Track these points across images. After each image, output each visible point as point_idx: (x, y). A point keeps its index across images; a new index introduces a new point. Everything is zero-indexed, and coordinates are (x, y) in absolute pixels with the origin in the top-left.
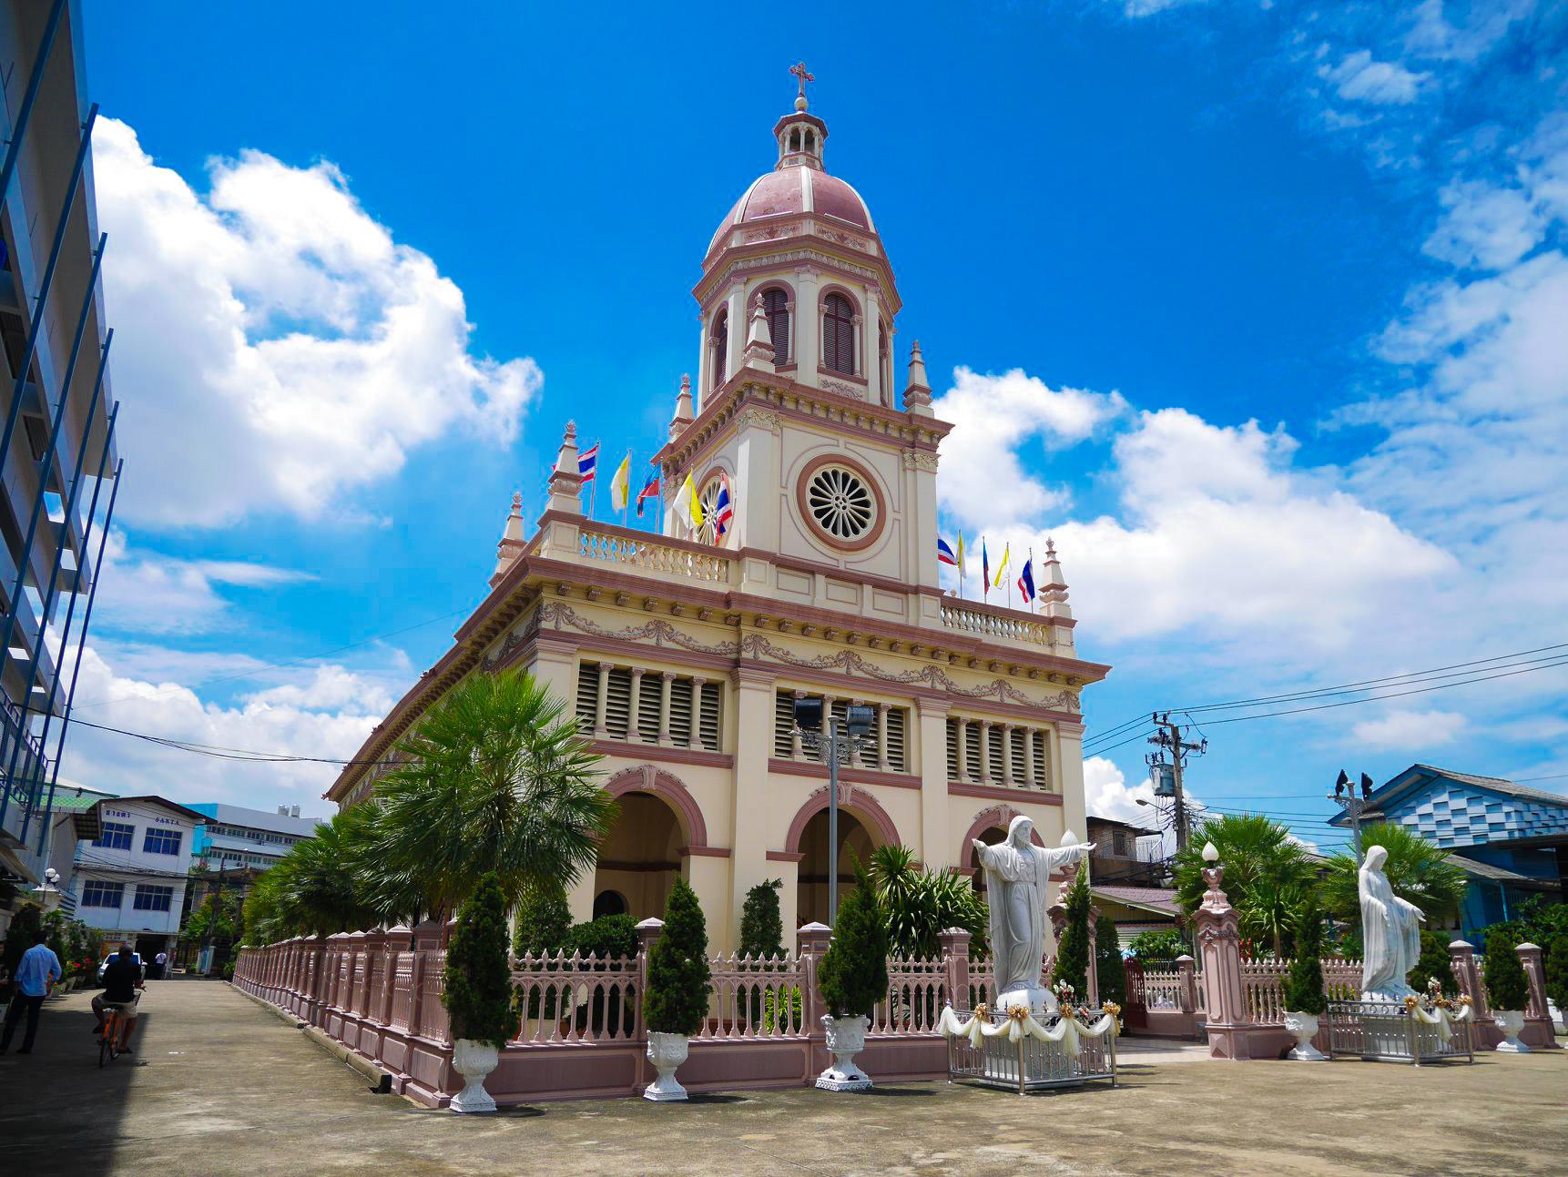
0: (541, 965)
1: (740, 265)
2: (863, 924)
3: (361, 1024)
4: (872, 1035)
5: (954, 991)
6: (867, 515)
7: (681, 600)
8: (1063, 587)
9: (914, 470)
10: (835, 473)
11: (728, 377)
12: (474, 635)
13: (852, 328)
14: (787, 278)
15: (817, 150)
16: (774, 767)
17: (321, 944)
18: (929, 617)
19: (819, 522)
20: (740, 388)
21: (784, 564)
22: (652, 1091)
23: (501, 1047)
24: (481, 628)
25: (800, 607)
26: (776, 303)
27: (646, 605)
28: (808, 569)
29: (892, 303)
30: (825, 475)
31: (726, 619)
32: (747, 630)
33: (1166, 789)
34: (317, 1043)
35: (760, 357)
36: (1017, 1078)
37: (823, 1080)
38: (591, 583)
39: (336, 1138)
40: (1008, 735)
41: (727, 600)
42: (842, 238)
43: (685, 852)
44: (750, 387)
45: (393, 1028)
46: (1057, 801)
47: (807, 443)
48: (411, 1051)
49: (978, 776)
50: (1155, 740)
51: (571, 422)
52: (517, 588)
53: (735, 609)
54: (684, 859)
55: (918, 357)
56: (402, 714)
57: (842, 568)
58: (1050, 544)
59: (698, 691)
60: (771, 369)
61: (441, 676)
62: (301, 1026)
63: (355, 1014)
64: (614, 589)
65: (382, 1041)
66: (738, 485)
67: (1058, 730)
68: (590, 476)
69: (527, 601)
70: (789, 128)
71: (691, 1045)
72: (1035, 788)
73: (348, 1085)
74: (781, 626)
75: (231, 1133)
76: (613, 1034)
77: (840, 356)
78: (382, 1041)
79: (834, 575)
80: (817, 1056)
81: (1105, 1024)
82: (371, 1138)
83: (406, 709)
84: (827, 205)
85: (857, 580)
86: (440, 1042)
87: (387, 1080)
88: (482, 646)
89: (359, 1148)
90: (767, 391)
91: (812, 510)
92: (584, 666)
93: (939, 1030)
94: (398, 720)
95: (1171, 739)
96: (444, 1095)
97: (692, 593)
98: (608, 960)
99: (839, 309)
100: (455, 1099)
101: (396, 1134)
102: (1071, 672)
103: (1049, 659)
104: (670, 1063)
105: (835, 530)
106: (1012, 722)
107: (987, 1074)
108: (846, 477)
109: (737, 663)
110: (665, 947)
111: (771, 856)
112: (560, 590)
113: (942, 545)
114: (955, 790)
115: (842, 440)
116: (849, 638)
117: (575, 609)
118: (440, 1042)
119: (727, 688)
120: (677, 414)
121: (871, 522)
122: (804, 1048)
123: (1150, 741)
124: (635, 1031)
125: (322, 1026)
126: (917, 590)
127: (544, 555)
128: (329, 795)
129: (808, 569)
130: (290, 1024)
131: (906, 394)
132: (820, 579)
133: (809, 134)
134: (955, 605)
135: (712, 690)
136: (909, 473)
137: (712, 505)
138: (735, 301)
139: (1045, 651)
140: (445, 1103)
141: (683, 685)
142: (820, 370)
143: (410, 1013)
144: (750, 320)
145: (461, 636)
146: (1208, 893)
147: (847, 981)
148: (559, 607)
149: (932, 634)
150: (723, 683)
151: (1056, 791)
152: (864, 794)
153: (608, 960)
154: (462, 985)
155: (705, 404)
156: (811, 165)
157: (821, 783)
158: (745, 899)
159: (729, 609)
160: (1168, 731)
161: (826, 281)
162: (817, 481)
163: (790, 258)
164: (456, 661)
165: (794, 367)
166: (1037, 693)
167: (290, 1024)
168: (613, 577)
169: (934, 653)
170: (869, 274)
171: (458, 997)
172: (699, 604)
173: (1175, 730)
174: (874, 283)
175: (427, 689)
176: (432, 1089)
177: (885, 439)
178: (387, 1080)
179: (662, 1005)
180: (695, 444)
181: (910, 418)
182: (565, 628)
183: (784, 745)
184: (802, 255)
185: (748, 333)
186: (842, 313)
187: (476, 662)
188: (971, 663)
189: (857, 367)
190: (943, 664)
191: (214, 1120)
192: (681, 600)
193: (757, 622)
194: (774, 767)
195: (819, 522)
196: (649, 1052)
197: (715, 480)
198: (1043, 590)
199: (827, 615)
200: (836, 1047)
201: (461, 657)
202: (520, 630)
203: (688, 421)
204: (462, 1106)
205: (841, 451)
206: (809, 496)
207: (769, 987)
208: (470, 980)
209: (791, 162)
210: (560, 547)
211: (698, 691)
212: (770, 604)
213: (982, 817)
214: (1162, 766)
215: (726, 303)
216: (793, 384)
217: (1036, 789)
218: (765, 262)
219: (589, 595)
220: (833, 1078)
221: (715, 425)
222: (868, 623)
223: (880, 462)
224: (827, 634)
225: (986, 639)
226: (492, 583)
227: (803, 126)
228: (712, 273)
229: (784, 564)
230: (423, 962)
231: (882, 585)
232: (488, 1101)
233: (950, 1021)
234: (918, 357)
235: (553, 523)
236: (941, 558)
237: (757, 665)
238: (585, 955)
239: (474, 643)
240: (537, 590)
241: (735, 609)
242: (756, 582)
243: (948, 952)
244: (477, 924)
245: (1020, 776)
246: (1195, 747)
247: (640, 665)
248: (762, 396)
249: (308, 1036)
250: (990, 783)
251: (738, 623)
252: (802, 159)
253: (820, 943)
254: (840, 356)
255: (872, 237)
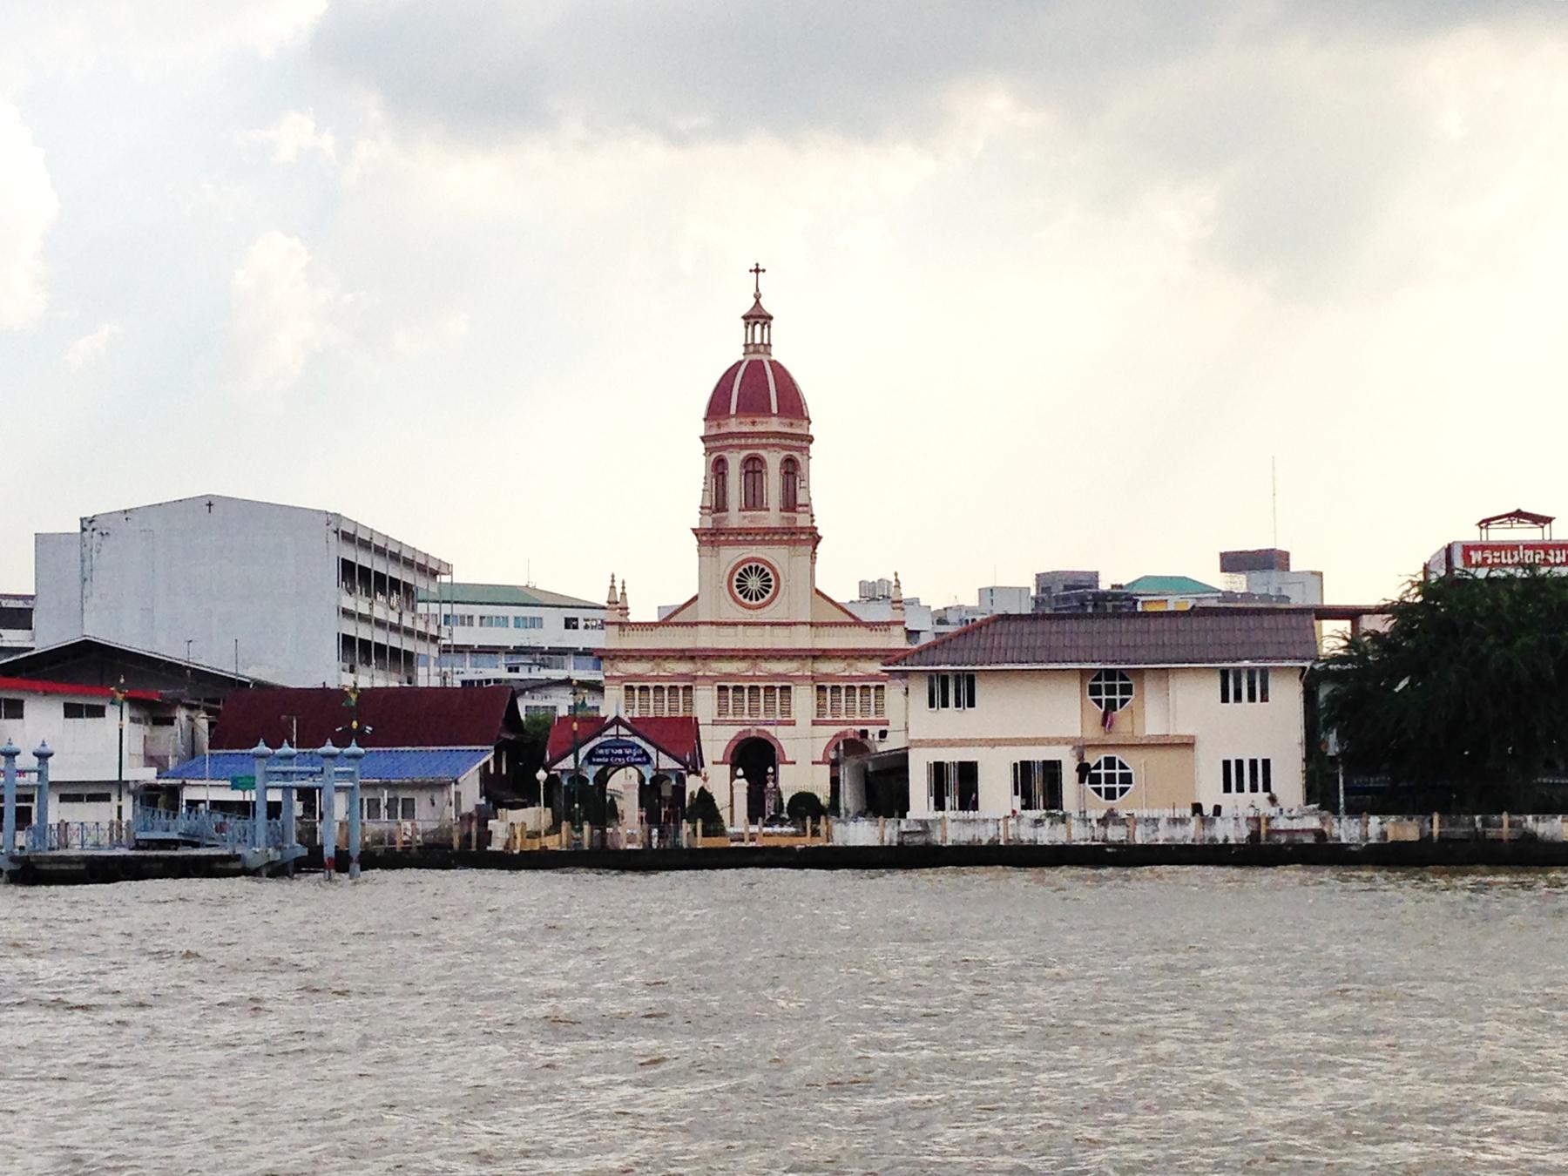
14: (725, 454)
18: (803, 639)
42: (753, 423)
79: (745, 624)
92: (627, 688)
99: (754, 467)
135: (688, 689)
157: (741, 728)
161: (745, 453)
177: (780, 542)
190: (809, 663)
223: (775, 555)
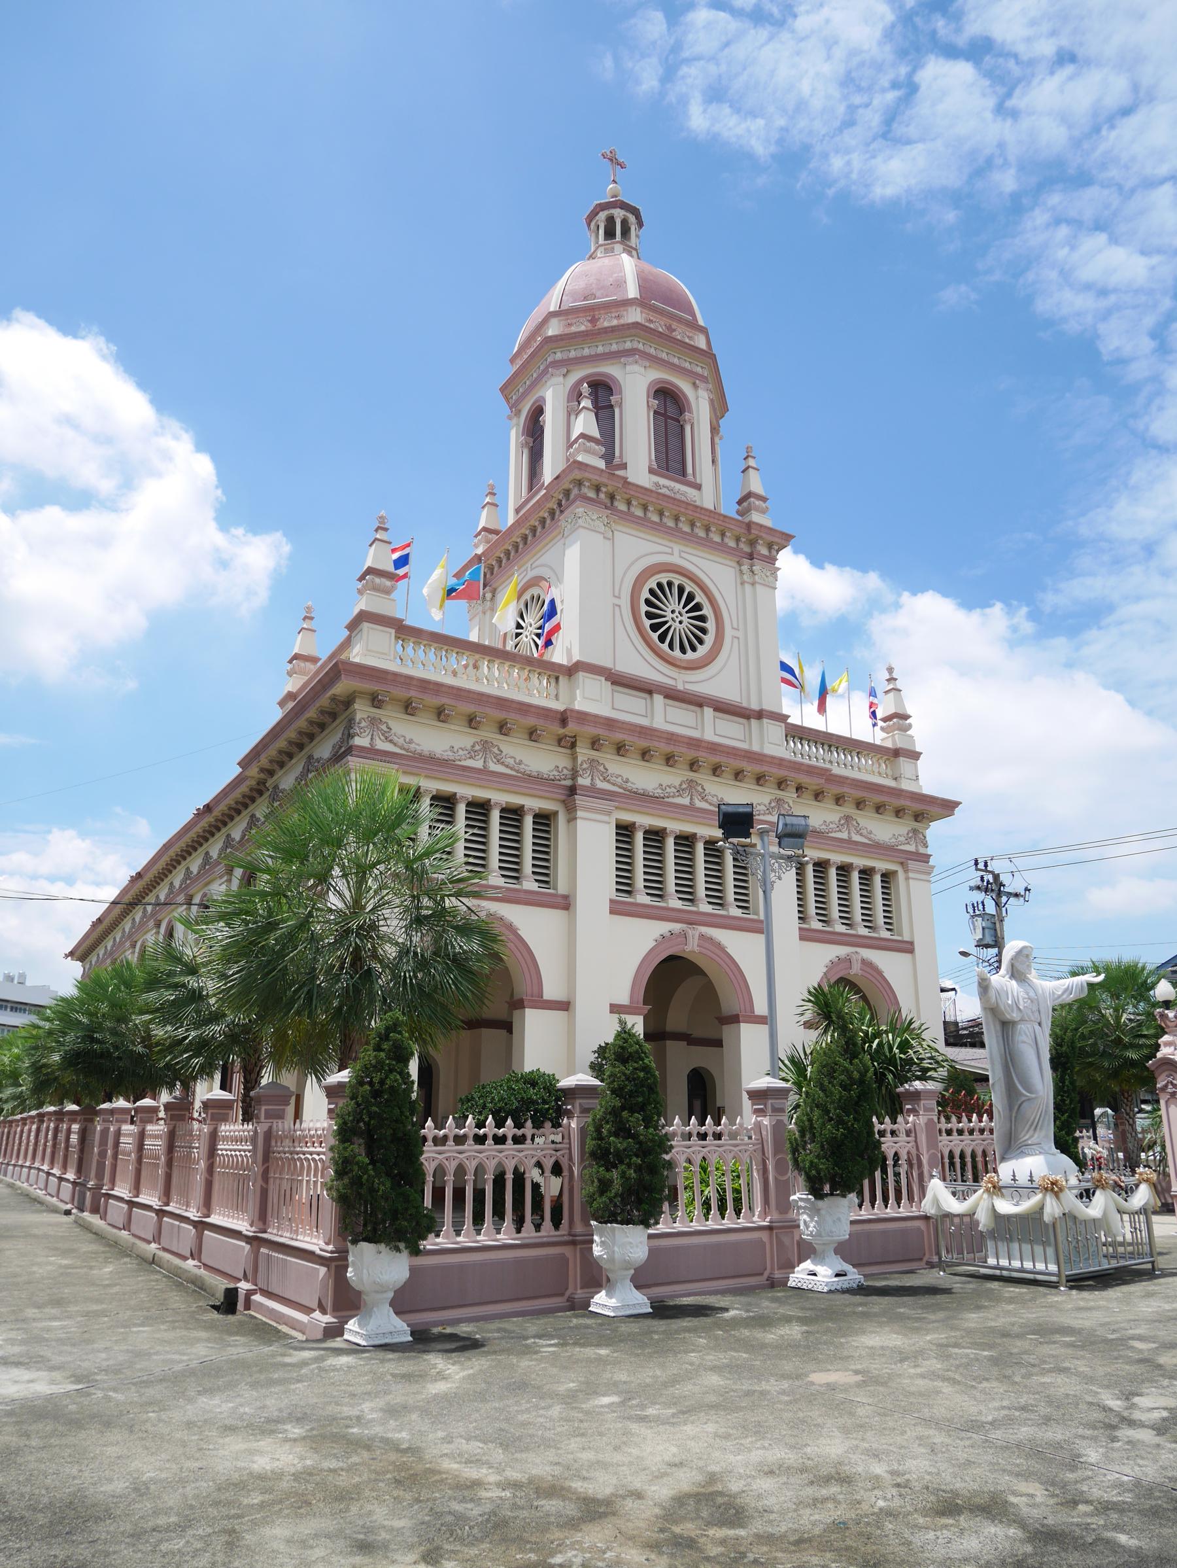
0: (445, 1137)
1: (559, 356)
2: (850, 1077)
3: (132, 1204)
4: (865, 1214)
5: (925, 1160)
6: (704, 631)
7: (511, 717)
8: (907, 717)
9: (753, 584)
10: (670, 584)
11: (548, 476)
12: (264, 761)
13: (682, 428)
15: (633, 241)
16: (616, 909)
17: (88, 1114)
19: (655, 636)
20: (566, 486)
21: (619, 681)
22: (603, 1302)
23: (415, 1251)
24: (272, 752)
25: (642, 727)
26: (602, 394)
27: (472, 722)
28: (646, 689)
29: (720, 407)
30: (660, 585)
31: (560, 741)
32: (584, 753)
33: (989, 940)
34: (98, 1235)
35: (588, 451)
36: (1053, 1268)
37: (800, 1276)
38: (412, 693)
39: (219, 1405)
40: (855, 876)
41: (563, 718)
42: (669, 328)
43: (518, 1005)
44: (579, 483)
45: (214, 1219)
46: (907, 948)
47: (640, 550)
48: (256, 1254)
49: (825, 919)
50: (978, 888)
51: (383, 513)
52: (324, 701)
53: (572, 727)
54: (516, 1013)
55: (751, 462)
56: (166, 859)
57: (680, 687)
58: (890, 670)
59: (528, 822)
60: (601, 464)
61: (217, 812)
62: (68, 1213)
63: (150, 1198)
64: (436, 701)
65: (200, 1237)
66: (567, 593)
67: (906, 871)
68: (405, 576)
69: (334, 716)
70: (602, 216)
71: (650, 1236)
72: (886, 934)
73: (177, 1300)
74: (620, 749)
75: (50, 1398)
76: (538, 1227)
77: (671, 454)
78: (200, 1237)
79: (673, 695)
80: (780, 1243)
81: (1142, 1196)
82: (274, 1402)
83: (172, 853)
84: (654, 295)
85: (697, 702)
86: (316, 1242)
87: (231, 1294)
88: (271, 773)
89: (266, 1427)
90: (598, 489)
91: (647, 623)
93: (927, 1206)
94: (161, 864)
95: (994, 887)
96: (328, 1318)
97: (524, 708)
98: (528, 1129)
99: (669, 405)
100: (352, 1325)
101: (303, 1393)
102: (918, 807)
103: (898, 793)
104: (627, 1265)
105: (671, 646)
106: (860, 862)
107: (992, 1261)
108: (681, 590)
109: (572, 790)
110: (614, 1112)
111: (615, 1009)
112: (376, 701)
113: (785, 667)
114: (806, 935)
115: (677, 548)
116: (693, 765)
117: (391, 723)
118: (316, 1242)
119: (562, 819)
120: (482, 524)
121: (709, 639)
122: (764, 1236)
123: (971, 889)
124: (565, 1221)
125: (95, 1210)
126: (760, 715)
127: (357, 660)
128: (71, 954)
129: (646, 689)
130: (55, 1210)
131: (739, 503)
132: (658, 699)
133: (625, 222)
134: (799, 733)
135: (544, 820)
136: (748, 587)
137: (532, 620)
138: (552, 396)
139: (892, 784)
140: (333, 1332)
141: (512, 815)
142: (651, 471)
143: (253, 1203)
144: (572, 412)
145: (245, 763)
146: (1166, 1038)
147: (835, 1150)
148: (374, 722)
149: (780, 762)
150: (556, 813)
151: (906, 938)
152: (711, 940)
153: (528, 1129)
154: (363, 1168)
155: (517, 511)
156: (629, 250)
157: (664, 927)
158: (592, 1057)
159: (565, 729)
160: (990, 878)
161: (656, 374)
162: (652, 591)
163: (614, 347)
164: (237, 794)
165: (624, 466)
166: (885, 830)
167: (55, 1210)
168: (436, 688)
169: (781, 784)
170: (699, 370)
171: (357, 1182)
172: (531, 721)
173: (996, 877)
174: (704, 379)
175: (198, 829)
176: (308, 1310)
177: (721, 548)
178: (231, 1294)
179: (617, 1187)
180: (508, 553)
181: (749, 526)
182: (381, 745)
183: (625, 884)
184: (628, 345)
185: (568, 428)
186: (672, 411)
187: (261, 793)
188: (818, 796)
189: (689, 470)
190: (790, 795)
191: (16, 1373)
192: (511, 717)
193: (595, 744)
194: (616, 909)
195: (655, 636)
196: (597, 1250)
197: (535, 591)
198: (885, 720)
199: (672, 738)
200: (819, 1234)
201: (244, 788)
202: (324, 750)
203: (496, 532)
204: (367, 1337)
205: (675, 559)
206: (644, 608)
207: (689, 1161)
208: (373, 1162)
209: (606, 251)
210: (374, 651)
211: (528, 822)
212: (610, 723)
213: (833, 965)
214: (983, 915)
215: (543, 399)
216: (625, 480)
217: (886, 934)
218: (586, 352)
219: (408, 708)
220: (816, 1275)
221: (534, 530)
222: (714, 748)
223: (716, 573)
224: (669, 760)
225: (836, 770)
226: (282, 704)
227: (618, 214)
228: (524, 367)
229: (619, 681)
230: (268, 1135)
231: (724, 708)
232: (399, 1329)
233: (939, 1195)
234: (751, 462)
235: (366, 626)
236: (785, 681)
237: (595, 793)
238: (500, 1124)
239: (262, 770)
240: (347, 702)
241: (572, 727)
242: (591, 698)
243: (914, 1111)
244: (382, 1082)
245: (868, 919)
246: (1017, 895)
247: (466, 791)
248: (592, 494)
249: (86, 1227)
250: (840, 928)
251: (573, 745)
252: (618, 248)
253: (778, 1103)
254: (671, 454)
255: (703, 330)
